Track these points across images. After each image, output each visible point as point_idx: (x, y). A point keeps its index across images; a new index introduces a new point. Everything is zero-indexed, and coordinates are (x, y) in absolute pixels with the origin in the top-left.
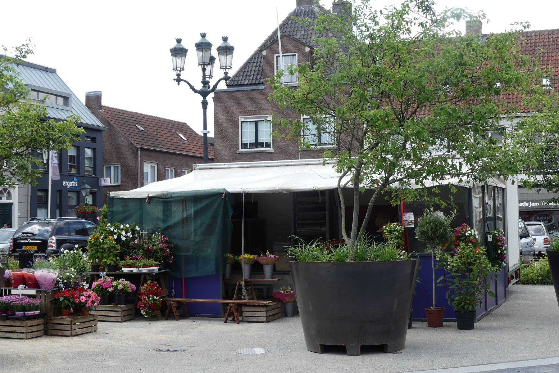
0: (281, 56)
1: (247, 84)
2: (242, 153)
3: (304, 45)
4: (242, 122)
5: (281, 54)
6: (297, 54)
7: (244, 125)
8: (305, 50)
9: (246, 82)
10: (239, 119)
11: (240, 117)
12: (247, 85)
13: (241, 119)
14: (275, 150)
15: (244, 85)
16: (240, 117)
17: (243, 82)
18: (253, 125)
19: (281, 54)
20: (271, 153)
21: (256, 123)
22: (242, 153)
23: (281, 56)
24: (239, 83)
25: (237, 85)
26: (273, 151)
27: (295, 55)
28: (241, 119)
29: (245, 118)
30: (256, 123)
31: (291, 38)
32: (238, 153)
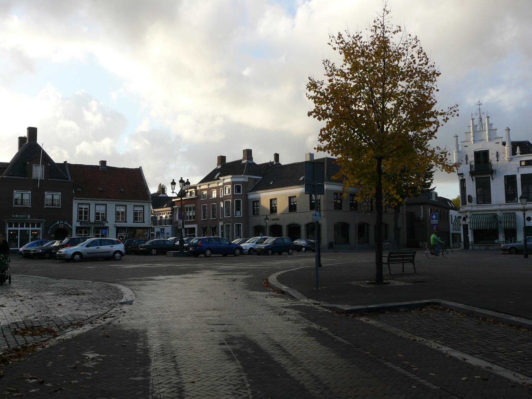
0: (40, 166)
2: (15, 207)
5: (40, 165)
9: (16, 174)
13: (15, 192)
18: (20, 195)
19: (40, 165)
21: (22, 194)
23: (40, 166)
28: (15, 192)
29: (17, 191)
30: (22, 194)
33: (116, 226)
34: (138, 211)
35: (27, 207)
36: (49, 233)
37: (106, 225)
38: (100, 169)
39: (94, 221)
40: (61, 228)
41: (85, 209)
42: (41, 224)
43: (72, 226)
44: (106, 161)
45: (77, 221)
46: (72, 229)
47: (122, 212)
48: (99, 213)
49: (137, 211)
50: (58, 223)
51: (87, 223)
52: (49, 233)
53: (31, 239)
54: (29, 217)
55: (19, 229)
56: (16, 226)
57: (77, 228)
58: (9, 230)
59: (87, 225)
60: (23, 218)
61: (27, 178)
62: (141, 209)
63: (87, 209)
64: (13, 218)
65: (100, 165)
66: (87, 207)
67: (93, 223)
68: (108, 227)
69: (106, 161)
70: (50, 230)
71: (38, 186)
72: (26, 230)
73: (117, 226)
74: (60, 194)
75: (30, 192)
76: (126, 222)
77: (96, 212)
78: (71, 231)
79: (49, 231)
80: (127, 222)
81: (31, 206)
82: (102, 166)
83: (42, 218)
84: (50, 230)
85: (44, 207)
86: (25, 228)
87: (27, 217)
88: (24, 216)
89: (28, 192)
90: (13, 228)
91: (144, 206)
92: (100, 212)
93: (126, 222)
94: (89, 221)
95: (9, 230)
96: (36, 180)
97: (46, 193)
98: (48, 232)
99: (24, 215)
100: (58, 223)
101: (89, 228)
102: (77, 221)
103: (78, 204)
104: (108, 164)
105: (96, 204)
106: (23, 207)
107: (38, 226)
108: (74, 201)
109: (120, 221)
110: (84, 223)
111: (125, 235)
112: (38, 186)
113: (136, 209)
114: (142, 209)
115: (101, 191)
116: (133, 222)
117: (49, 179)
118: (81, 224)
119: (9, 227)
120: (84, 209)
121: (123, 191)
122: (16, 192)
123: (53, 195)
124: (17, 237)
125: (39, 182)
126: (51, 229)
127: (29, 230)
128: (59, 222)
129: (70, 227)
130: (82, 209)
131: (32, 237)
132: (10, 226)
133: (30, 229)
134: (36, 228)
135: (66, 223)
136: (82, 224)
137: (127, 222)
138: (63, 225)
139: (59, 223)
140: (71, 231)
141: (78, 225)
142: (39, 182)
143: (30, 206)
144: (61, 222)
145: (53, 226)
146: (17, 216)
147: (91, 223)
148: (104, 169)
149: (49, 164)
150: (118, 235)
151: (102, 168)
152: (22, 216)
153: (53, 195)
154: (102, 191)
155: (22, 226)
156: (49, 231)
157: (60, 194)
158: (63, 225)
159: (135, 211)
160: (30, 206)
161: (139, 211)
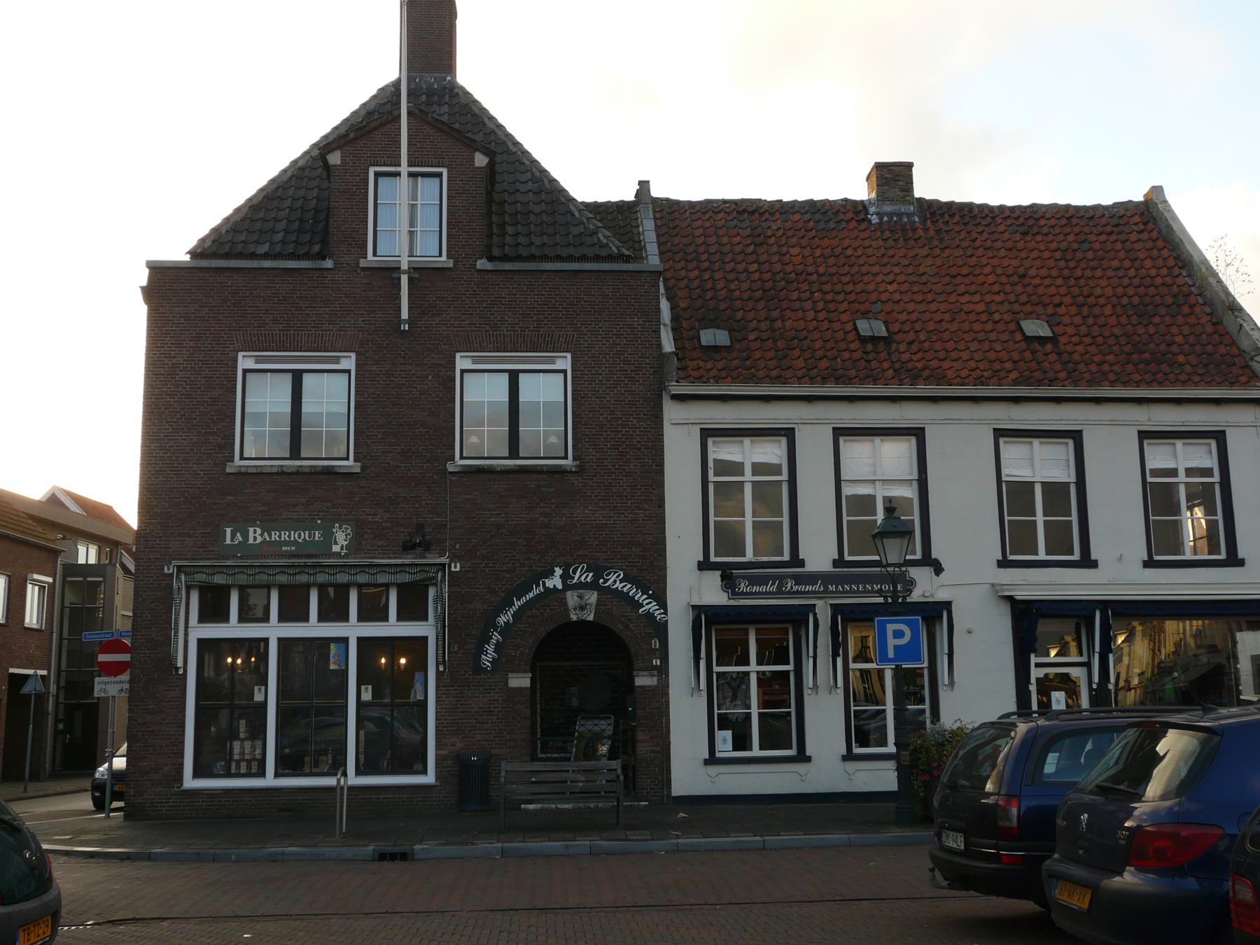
1: (266, 253)
3: (473, 147)
4: (245, 371)
6: (445, 171)
7: (249, 376)
8: (473, 159)
9: (264, 248)
10: (236, 361)
11: (241, 355)
12: (266, 256)
13: (245, 361)
14: (363, 468)
15: (253, 256)
16: (241, 355)
17: (252, 248)
18: (286, 382)
20: (349, 475)
21: (297, 377)
22: (246, 474)
24: (239, 248)
25: (227, 256)
26: (358, 470)
27: (439, 175)
28: (245, 361)
29: (258, 360)
30: (297, 377)
31: (428, 123)
32: (228, 470)
33: (1010, 599)
34: (1182, 477)
35: (329, 471)
36: (487, 659)
37: (925, 587)
38: (875, 219)
39: (836, 563)
40: (582, 623)
41: (758, 468)
42: (432, 592)
43: (663, 605)
44: (909, 166)
45: (704, 565)
46: (661, 630)
47: (1055, 492)
48: (871, 499)
49: (1173, 472)
50: (555, 582)
51: (782, 578)
52: (487, 659)
53: (360, 704)
54: (341, 539)
55: (274, 631)
56: (334, 611)
57: (705, 618)
58: (201, 642)
59: (780, 593)
60: (302, 551)
61: (329, 264)
62: (1201, 456)
63: (774, 469)
64: (230, 552)
65: (873, 195)
66: (772, 452)
67: (825, 578)
68: (947, 605)
69: (909, 166)
70: (496, 637)
71: (405, 315)
72: (325, 642)
73: (1021, 594)
74: (564, 362)
75: (349, 362)
76: (1087, 562)
77: (848, 490)
78: (656, 644)
79: (490, 649)
80: (1094, 564)
81: (355, 461)
82: (882, 197)
83: (426, 547)
84: (496, 637)
85: (451, 468)
86: (314, 628)
87: (329, 538)
88: (305, 535)
89: (336, 360)
90: (233, 629)
91: (1220, 437)
92: (881, 493)
93: (1087, 562)
94: (796, 561)
95: (201, 642)
96: (389, 273)
97: (462, 362)
98: (481, 651)
99: (311, 529)
100: (555, 582)
101: (799, 618)
102: (704, 565)
103: (706, 434)
104: (925, 187)
105: (840, 433)
106: (298, 473)
107: (412, 609)
108: (672, 412)
109: (1042, 556)
110: (754, 581)
111: (1088, 665)
112: (405, 315)
113: (1159, 457)
114: (1211, 462)
115: (874, 339)
116: (1149, 564)
117: (482, 264)
118: (729, 581)
119: (204, 617)
120: (748, 470)
121: (1042, 329)
122: (250, 364)
123: (514, 377)
124: (258, 697)
125: (404, 279)
126: (506, 630)
127: (345, 640)
128: (565, 577)
129: (649, 615)
130: (737, 468)
131: (367, 696)
132: (214, 610)
133: (354, 630)
134: (393, 628)
135: (614, 580)
136: (743, 587)
137: (1094, 564)
138: (592, 597)
139: (566, 587)
140: (656, 644)
141: (713, 593)
142: (404, 279)
143: (351, 462)
144: (581, 575)
145: (517, 604)
146: (255, 535)
147: (812, 578)
148: (900, 215)
149: (481, 160)
150: (1036, 673)
151: (888, 208)
152: (294, 536)
153: (514, 377)
154: (887, 340)
155: (294, 611)
156: (490, 649)
157: (564, 362)
158: (592, 597)
159: (1157, 472)
160: (351, 462)
161: (1190, 472)
